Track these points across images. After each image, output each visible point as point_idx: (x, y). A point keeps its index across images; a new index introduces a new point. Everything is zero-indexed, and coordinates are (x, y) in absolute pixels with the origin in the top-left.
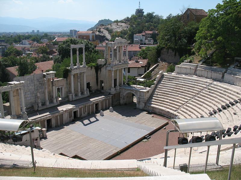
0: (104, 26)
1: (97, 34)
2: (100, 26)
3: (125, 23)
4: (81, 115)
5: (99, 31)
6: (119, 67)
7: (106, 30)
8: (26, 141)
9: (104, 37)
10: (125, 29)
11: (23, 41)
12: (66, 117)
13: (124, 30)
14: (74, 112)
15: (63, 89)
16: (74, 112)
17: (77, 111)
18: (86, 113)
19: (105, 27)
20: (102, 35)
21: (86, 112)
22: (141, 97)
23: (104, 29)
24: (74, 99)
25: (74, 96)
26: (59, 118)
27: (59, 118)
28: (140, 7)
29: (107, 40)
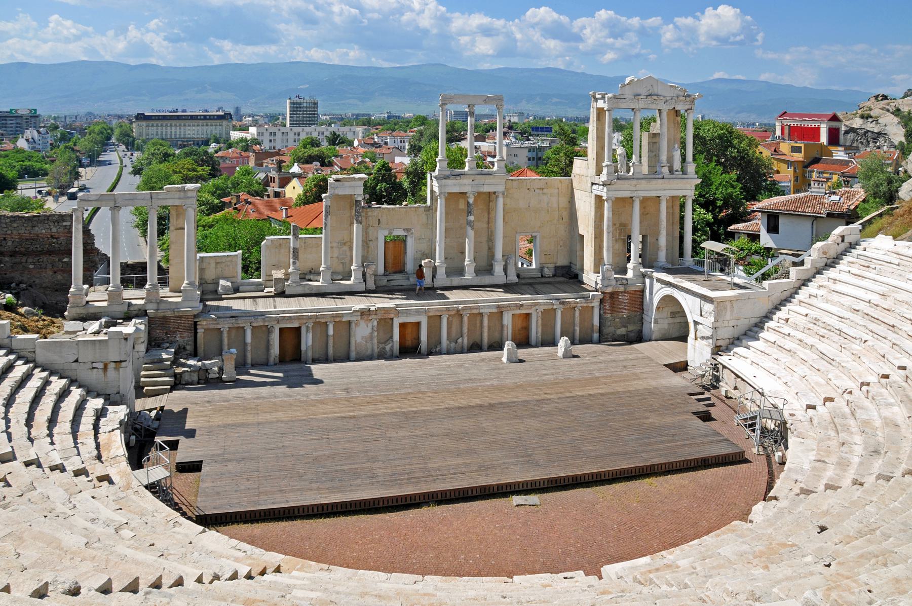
0: (886, 101)
1: (854, 126)
2: (873, 100)
7: (892, 113)
8: (76, 361)
12: (362, 333)
14: (403, 326)
15: (410, 241)
16: (403, 326)
17: (418, 324)
18: (460, 340)
19: (888, 104)
20: (876, 130)
22: (699, 319)
23: (882, 109)
25: (441, 272)
26: (331, 331)
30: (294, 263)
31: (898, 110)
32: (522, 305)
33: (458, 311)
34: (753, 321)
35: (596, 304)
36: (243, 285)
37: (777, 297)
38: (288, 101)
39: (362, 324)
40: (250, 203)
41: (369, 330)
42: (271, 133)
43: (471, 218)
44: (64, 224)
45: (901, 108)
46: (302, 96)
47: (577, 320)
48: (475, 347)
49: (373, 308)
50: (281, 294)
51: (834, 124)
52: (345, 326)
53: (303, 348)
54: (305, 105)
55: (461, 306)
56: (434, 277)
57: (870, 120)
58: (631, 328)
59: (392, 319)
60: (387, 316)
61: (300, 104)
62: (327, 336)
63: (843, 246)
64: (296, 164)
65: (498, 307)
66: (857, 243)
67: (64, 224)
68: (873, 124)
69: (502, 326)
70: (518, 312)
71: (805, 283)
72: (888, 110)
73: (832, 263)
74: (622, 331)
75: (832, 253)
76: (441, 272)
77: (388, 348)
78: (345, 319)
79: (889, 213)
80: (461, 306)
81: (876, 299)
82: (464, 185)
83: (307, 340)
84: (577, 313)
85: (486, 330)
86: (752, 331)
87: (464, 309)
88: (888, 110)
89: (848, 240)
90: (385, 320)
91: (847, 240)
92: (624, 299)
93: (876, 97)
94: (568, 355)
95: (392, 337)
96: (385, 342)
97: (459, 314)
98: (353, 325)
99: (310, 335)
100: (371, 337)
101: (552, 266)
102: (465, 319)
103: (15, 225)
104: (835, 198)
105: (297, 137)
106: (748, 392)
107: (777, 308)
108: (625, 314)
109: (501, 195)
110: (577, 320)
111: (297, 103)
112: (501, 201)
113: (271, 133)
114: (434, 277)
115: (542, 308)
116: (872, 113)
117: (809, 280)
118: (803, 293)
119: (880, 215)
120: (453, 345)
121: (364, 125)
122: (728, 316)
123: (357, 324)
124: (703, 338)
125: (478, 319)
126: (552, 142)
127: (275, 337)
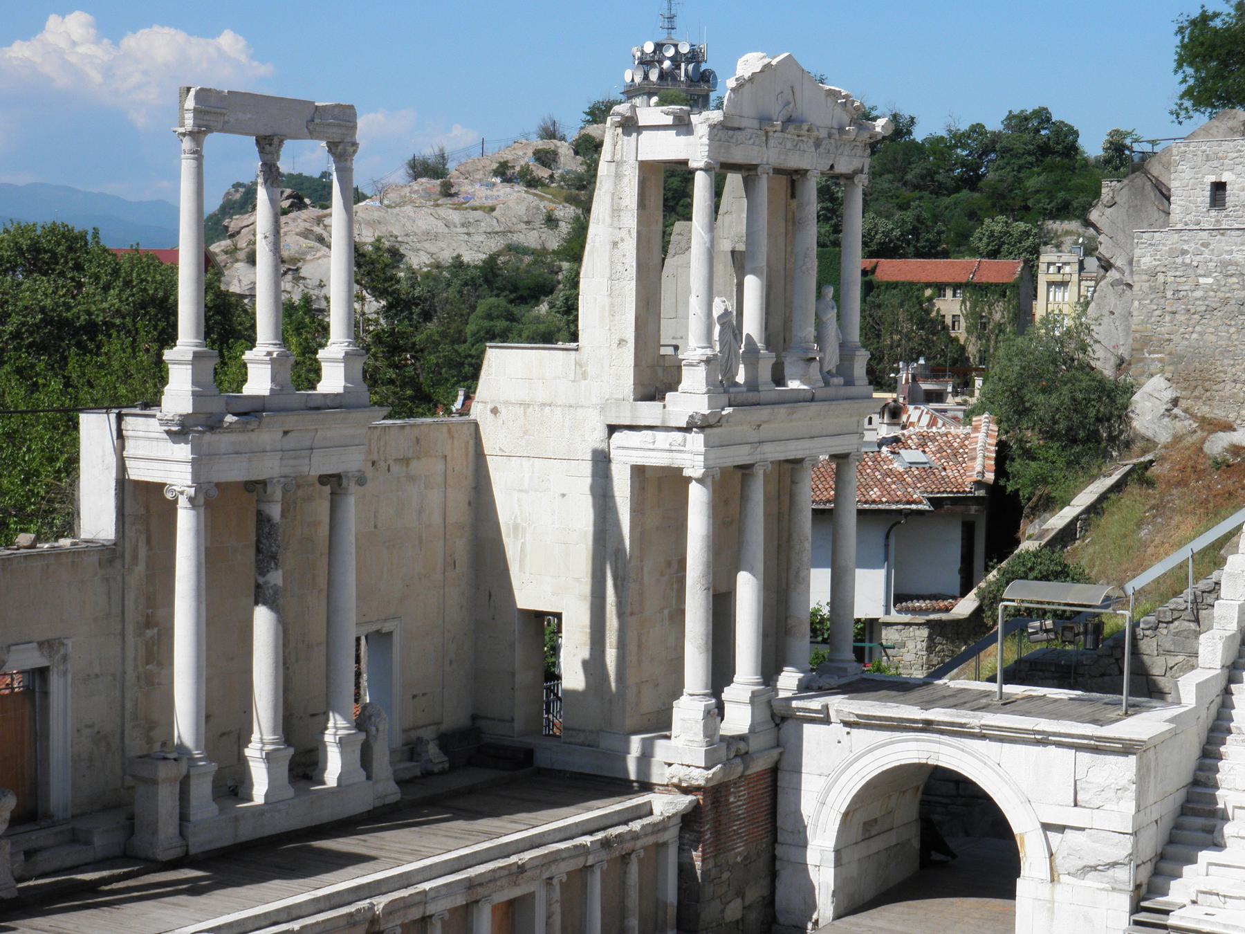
3: (532, 183)
6: (768, 431)
10: (530, 239)
13: (512, 249)
24: (200, 842)
28: (678, 22)
32: (521, 868)
35: (671, 835)
43: (276, 577)
55: (381, 902)
56: (184, 818)
65: (470, 884)
79: (1140, 476)
80: (381, 902)
82: (262, 457)
84: (634, 869)
87: (391, 909)
92: (737, 801)
101: (428, 733)
104: (911, 455)
108: (739, 849)
109: (353, 487)
114: (184, 818)
119: (1118, 487)
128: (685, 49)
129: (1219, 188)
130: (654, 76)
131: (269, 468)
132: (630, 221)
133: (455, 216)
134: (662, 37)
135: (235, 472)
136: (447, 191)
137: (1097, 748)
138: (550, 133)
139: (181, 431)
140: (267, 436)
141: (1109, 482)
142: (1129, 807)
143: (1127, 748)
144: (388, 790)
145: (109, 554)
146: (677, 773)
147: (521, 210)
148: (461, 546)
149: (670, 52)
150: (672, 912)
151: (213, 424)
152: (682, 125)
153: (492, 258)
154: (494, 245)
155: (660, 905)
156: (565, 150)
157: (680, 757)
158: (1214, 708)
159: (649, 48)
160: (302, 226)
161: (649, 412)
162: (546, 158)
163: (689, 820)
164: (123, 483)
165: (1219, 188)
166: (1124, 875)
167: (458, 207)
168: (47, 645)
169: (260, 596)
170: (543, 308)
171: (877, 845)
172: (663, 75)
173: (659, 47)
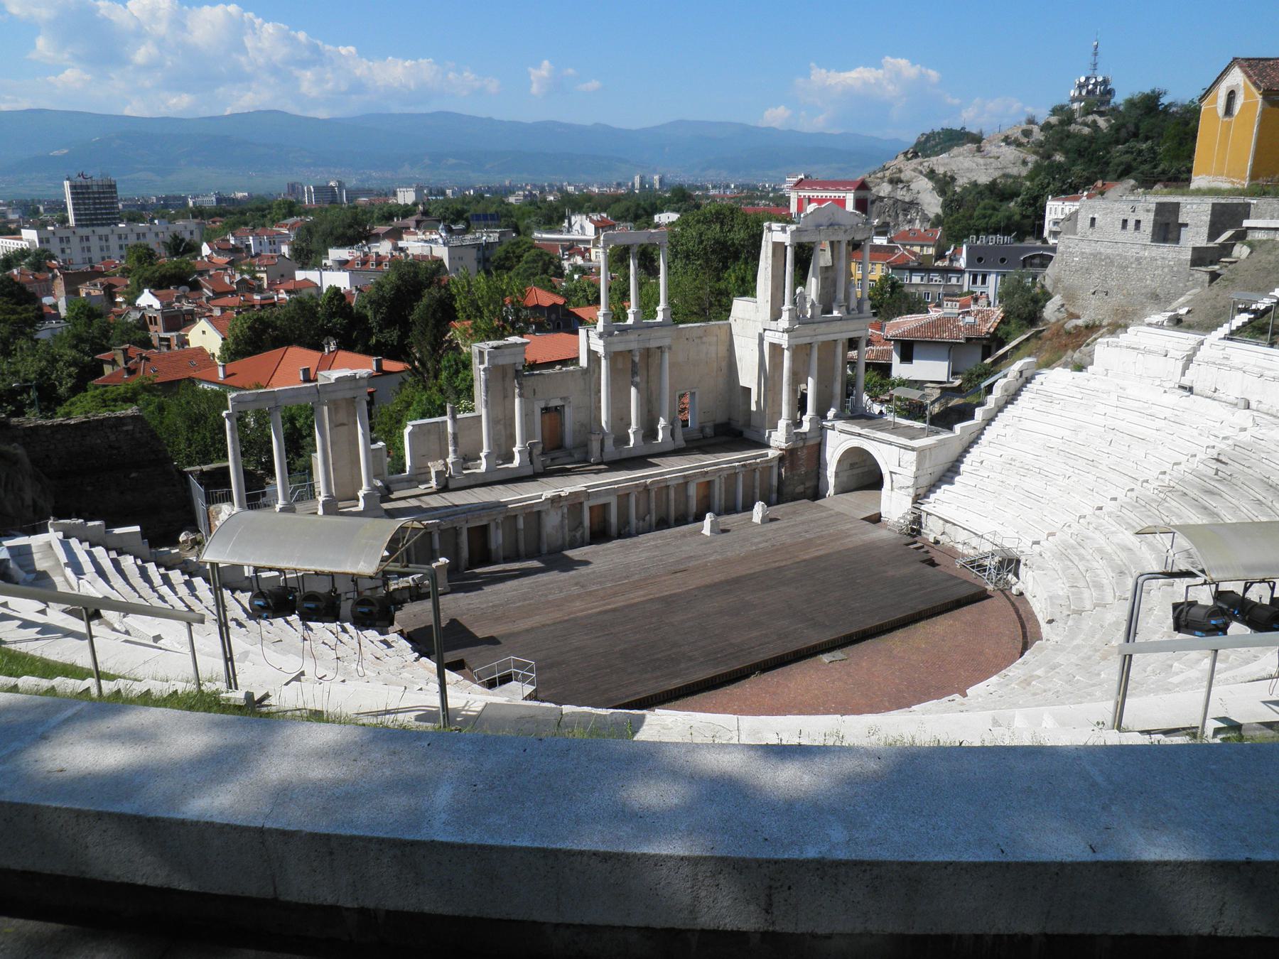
0: (919, 160)
1: (882, 194)
2: (901, 157)
3: (1019, 145)
4: (627, 523)
5: (894, 181)
6: (818, 331)
7: (926, 176)
9: (912, 204)
10: (1014, 171)
11: (573, 219)
12: (552, 521)
13: (1006, 176)
14: (591, 508)
16: (591, 508)
19: (921, 164)
20: (907, 199)
21: (649, 512)
23: (915, 170)
24: (606, 458)
26: (521, 524)
27: (521, 524)
29: (925, 218)
30: (455, 451)
31: (932, 171)
32: (707, 472)
33: (646, 486)
34: (946, 466)
35: (775, 463)
36: (391, 482)
37: (967, 439)
38: (67, 184)
39: (552, 512)
40: (148, 359)
41: (559, 518)
42: (61, 239)
43: (638, 379)
44: (125, 428)
45: (935, 168)
46: (89, 173)
47: (757, 483)
48: (663, 524)
49: (563, 494)
50: (444, 488)
51: (862, 193)
52: (534, 515)
53: (493, 546)
54: (95, 189)
55: (649, 481)
56: (602, 450)
57: (900, 186)
58: (808, 484)
59: (581, 504)
60: (577, 501)
61: (88, 187)
62: (517, 530)
63: (1021, 380)
64: (146, 291)
65: (685, 476)
66: (1033, 378)
67: (125, 428)
68: (904, 192)
69: (687, 497)
70: (702, 480)
71: (989, 421)
72: (921, 172)
73: (1012, 398)
74: (800, 489)
75: (1012, 390)
76: (609, 443)
77: (578, 535)
78: (535, 509)
79: (1037, 335)
80: (649, 481)
81: (1067, 433)
82: (632, 342)
83: (497, 539)
85: (672, 503)
86: (949, 473)
87: (652, 483)
88: (921, 172)
89: (1026, 374)
90: (574, 503)
91: (1024, 375)
92: (802, 454)
93: (906, 154)
94: (767, 520)
95: (581, 523)
96: (576, 529)
97: (646, 489)
98: (543, 515)
99: (500, 532)
100: (562, 526)
101: (711, 424)
102: (653, 494)
103: (59, 437)
105: (104, 243)
106: (962, 536)
107: (966, 451)
108: (803, 470)
110: (757, 483)
111: (81, 187)
112: (667, 356)
113: (61, 239)
114: (602, 450)
115: (725, 473)
116: (902, 176)
117: (992, 419)
118: (990, 433)
119: (1027, 339)
120: (641, 523)
121: (195, 217)
122: (927, 465)
123: (547, 512)
124: (901, 488)
125: (664, 492)
126: (502, 234)
127: (464, 538)
128: (1100, 79)
129: (1093, 219)
130: (1084, 93)
131: (633, 346)
132: (770, 262)
133: (981, 161)
134: (1090, 73)
135: (620, 348)
136: (979, 150)
137: (906, 448)
138: (1031, 121)
139: (601, 336)
140: (632, 336)
141: (1025, 337)
142: (914, 469)
143: (913, 449)
144: (681, 442)
145: (585, 372)
146: (777, 444)
147: (1012, 158)
148: (724, 364)
149: (1093, 81)
150: (775, 488)
151: (611, 334)
152: (784, 230)
153: (995, 180)
154: (997, 174)
155: (771, 485)
156: (1036, 129)
157: (779, 438)
158: (974, 436)
159: (1083, 79)
160: (914, 166)
161: (773, 325)
162: (1027, 133)
163: (781, 459)
164: (589, 350)
165: (1093, 219)
166: (911, 491)
167: (983, 157)
168: (563, 399)
169: (633, 383)
170: (1012, 204)
171: (856, 471)
172: (1088, 92)
173: (1088, 79)
